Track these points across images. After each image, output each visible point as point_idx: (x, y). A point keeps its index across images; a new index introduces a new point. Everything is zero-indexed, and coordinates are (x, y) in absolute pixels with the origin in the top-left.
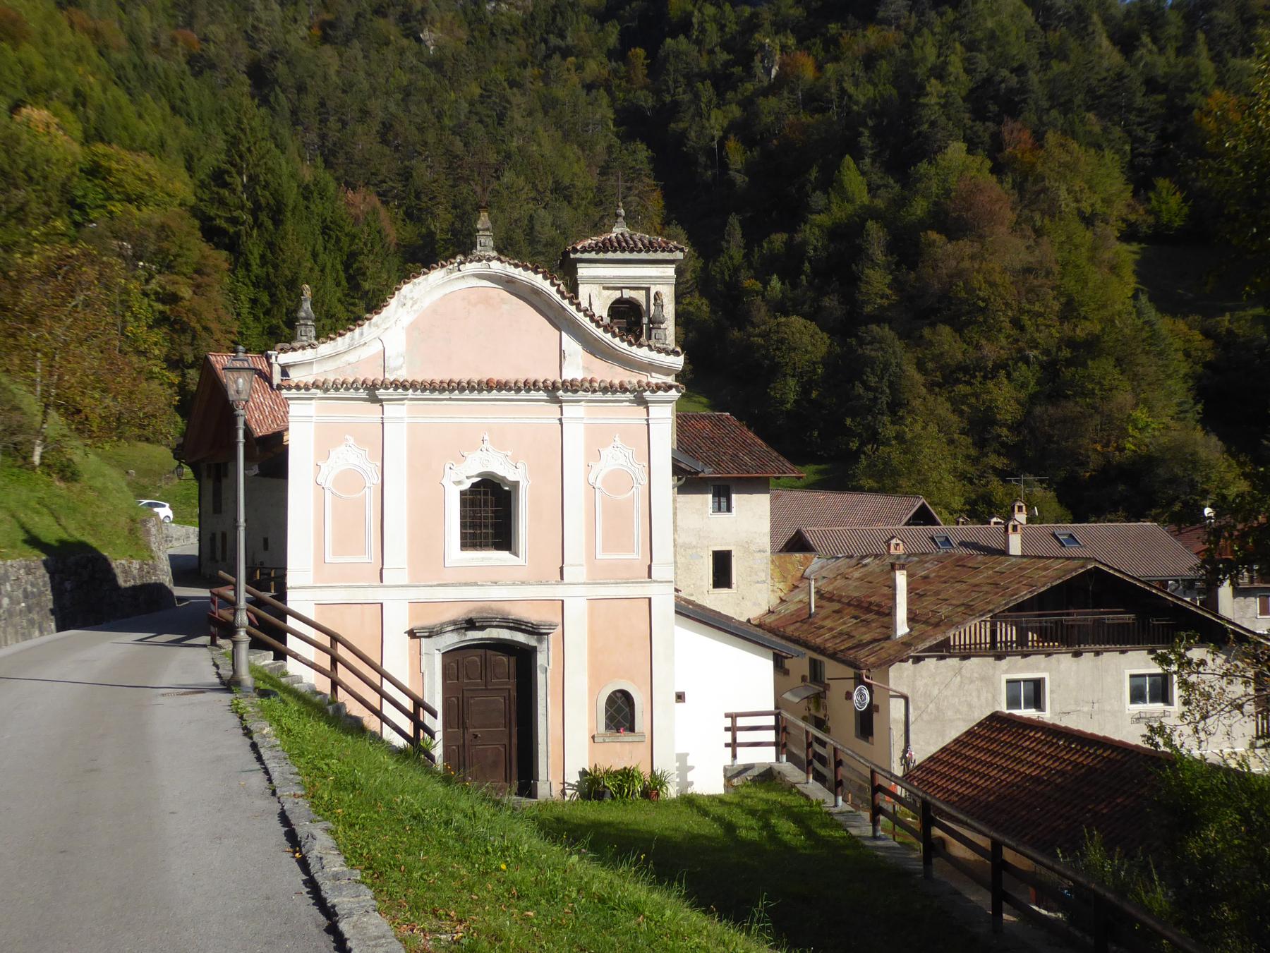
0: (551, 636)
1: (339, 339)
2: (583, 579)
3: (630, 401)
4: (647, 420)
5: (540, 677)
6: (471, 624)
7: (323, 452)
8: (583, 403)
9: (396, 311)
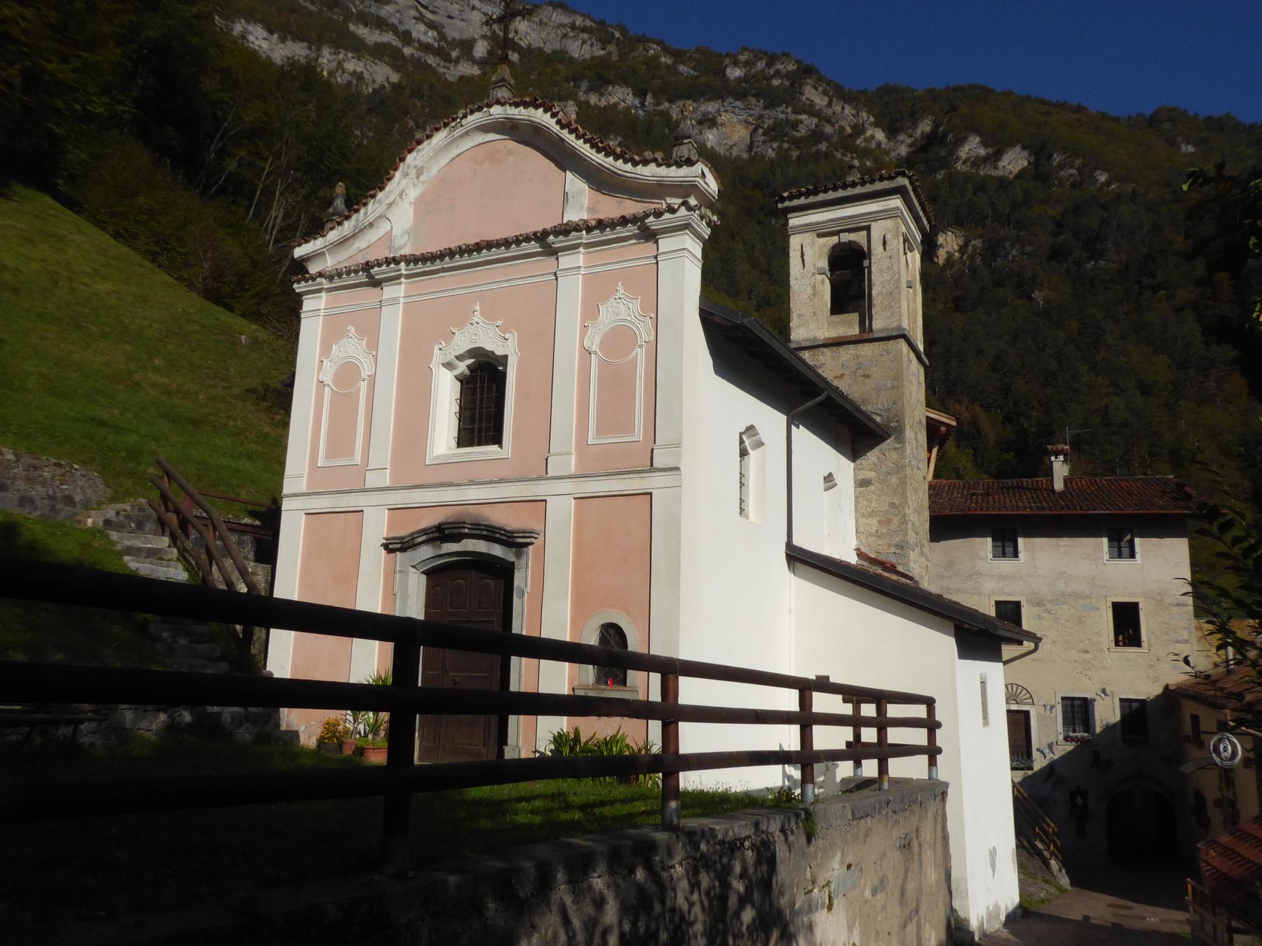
0: (530, 547)
1: (346, 223)
2: (572, 469)
3: (634, 237)
4: (656, 257)
5: (516, 601)
6: (442, 533)
7: (326, 351)
8: (581, 249)
9: (399, 183)
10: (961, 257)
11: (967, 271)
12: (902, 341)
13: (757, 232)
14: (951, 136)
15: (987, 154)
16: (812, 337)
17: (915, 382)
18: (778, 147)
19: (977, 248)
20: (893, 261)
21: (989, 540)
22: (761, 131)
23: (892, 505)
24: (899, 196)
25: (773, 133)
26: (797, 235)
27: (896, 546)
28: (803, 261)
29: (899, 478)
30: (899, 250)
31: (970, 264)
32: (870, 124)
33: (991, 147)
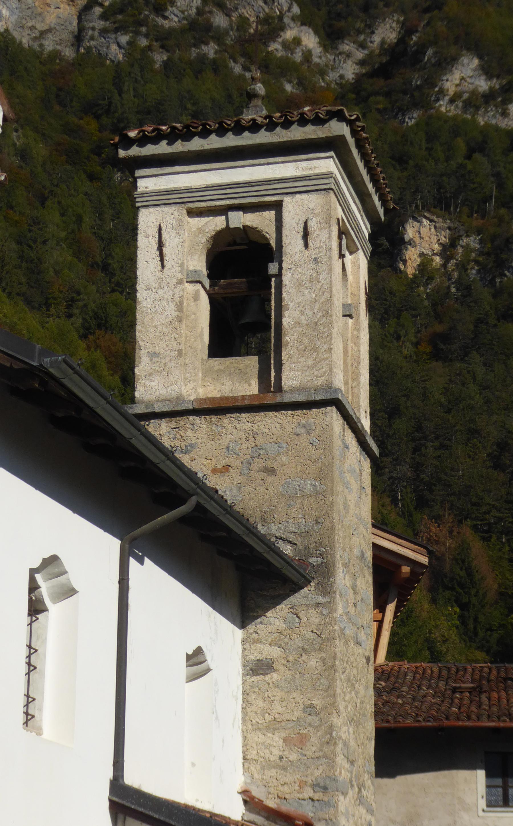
10: (445, 265)
11: (453, 290)
12: (333, 410)
13: (86, 194)
14: (430, 52)
15: (491, 88)
16: (174, 395)
17: (355, 486)
18: (129, 43)
19: (472, 251)
20: (321, 267)
21: (481, 774)
22: (98, 10)
23: (310, 709)
24: (332, 153)
25: (120, 17)
26: (151, 209)
27: (315, 786)
28: (161, 256)
29: (323, 661)
30: (330, 249)
31: (460, 277)
32: (293, 19)
33: (498, 77)
